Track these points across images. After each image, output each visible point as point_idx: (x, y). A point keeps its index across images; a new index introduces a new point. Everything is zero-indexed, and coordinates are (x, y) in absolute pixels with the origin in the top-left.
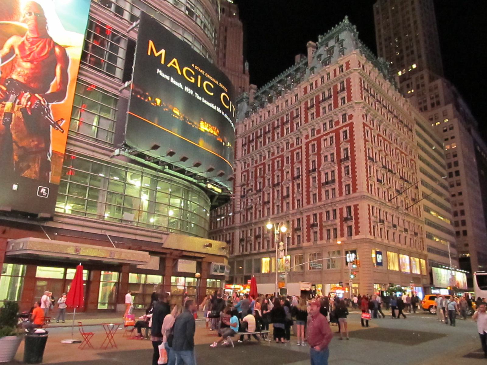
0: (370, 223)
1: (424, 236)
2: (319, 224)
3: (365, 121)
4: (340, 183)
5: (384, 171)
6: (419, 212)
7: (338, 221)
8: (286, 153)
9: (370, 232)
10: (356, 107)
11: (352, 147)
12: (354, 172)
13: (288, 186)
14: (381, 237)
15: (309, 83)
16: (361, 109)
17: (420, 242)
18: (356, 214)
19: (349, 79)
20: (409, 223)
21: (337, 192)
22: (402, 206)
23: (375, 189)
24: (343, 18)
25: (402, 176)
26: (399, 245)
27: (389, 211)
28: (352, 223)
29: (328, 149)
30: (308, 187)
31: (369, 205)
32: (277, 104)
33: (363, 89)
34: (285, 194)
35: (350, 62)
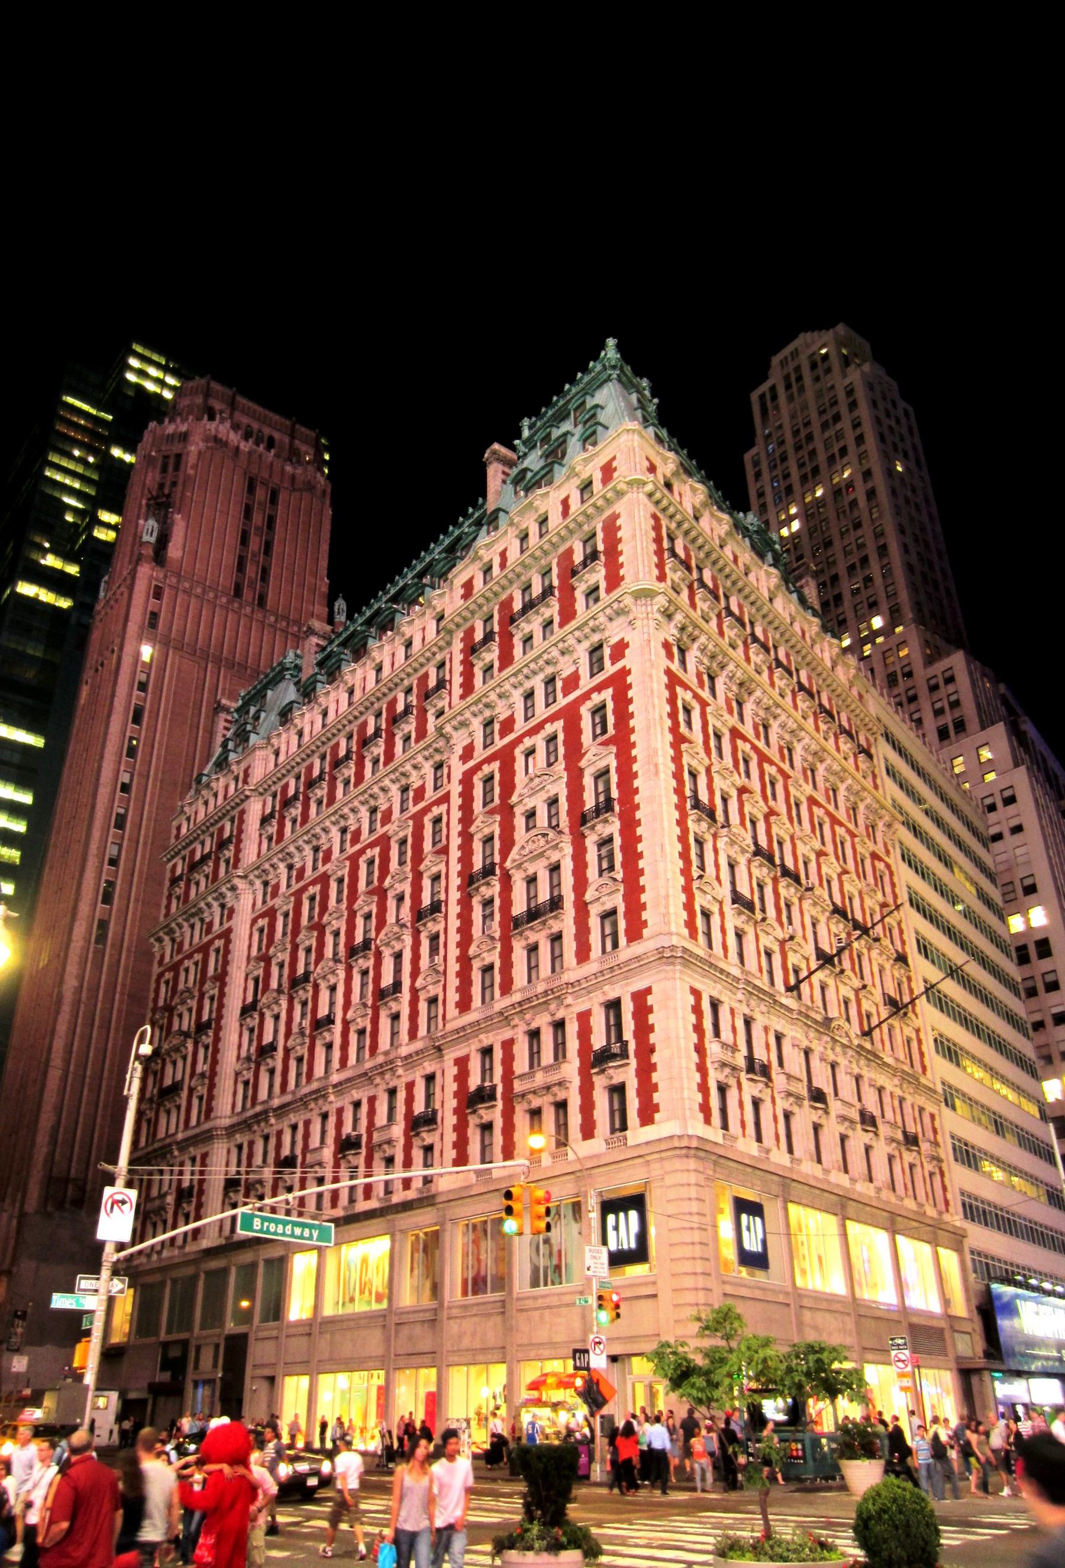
0: (702, 1068)
1: (946, 1152)
2: (500, 1090)
3: (675, 666)
4: (582, 909)
5: (761, 871)
6: (916, 1056)
7: (571, 1069)
8: (399, 828)
9: (705, 1108)
10: (638, 610)
11: (626, 761)
12: (632, 856)
13: (398, 947)
14: (759, 1139)
15: (478, 565)
16: (658, 616)
17: (931, 1174)
18: (644, 1029)
19: (615, 517)
20: (880, 1090)
21: (569, 945)
22: (848, 1020)
23: (723, 931)
24: (603, 346)
25: (839, 903)
26: (843, 1180)
27: (794, 1033)
28: (627, 1074)
29: (539, 785)
30: (465, 942)
31: (696, 993)
32: (378, 661)
33: (666, 555)
34: (387, 980)
35: (614, 464)
